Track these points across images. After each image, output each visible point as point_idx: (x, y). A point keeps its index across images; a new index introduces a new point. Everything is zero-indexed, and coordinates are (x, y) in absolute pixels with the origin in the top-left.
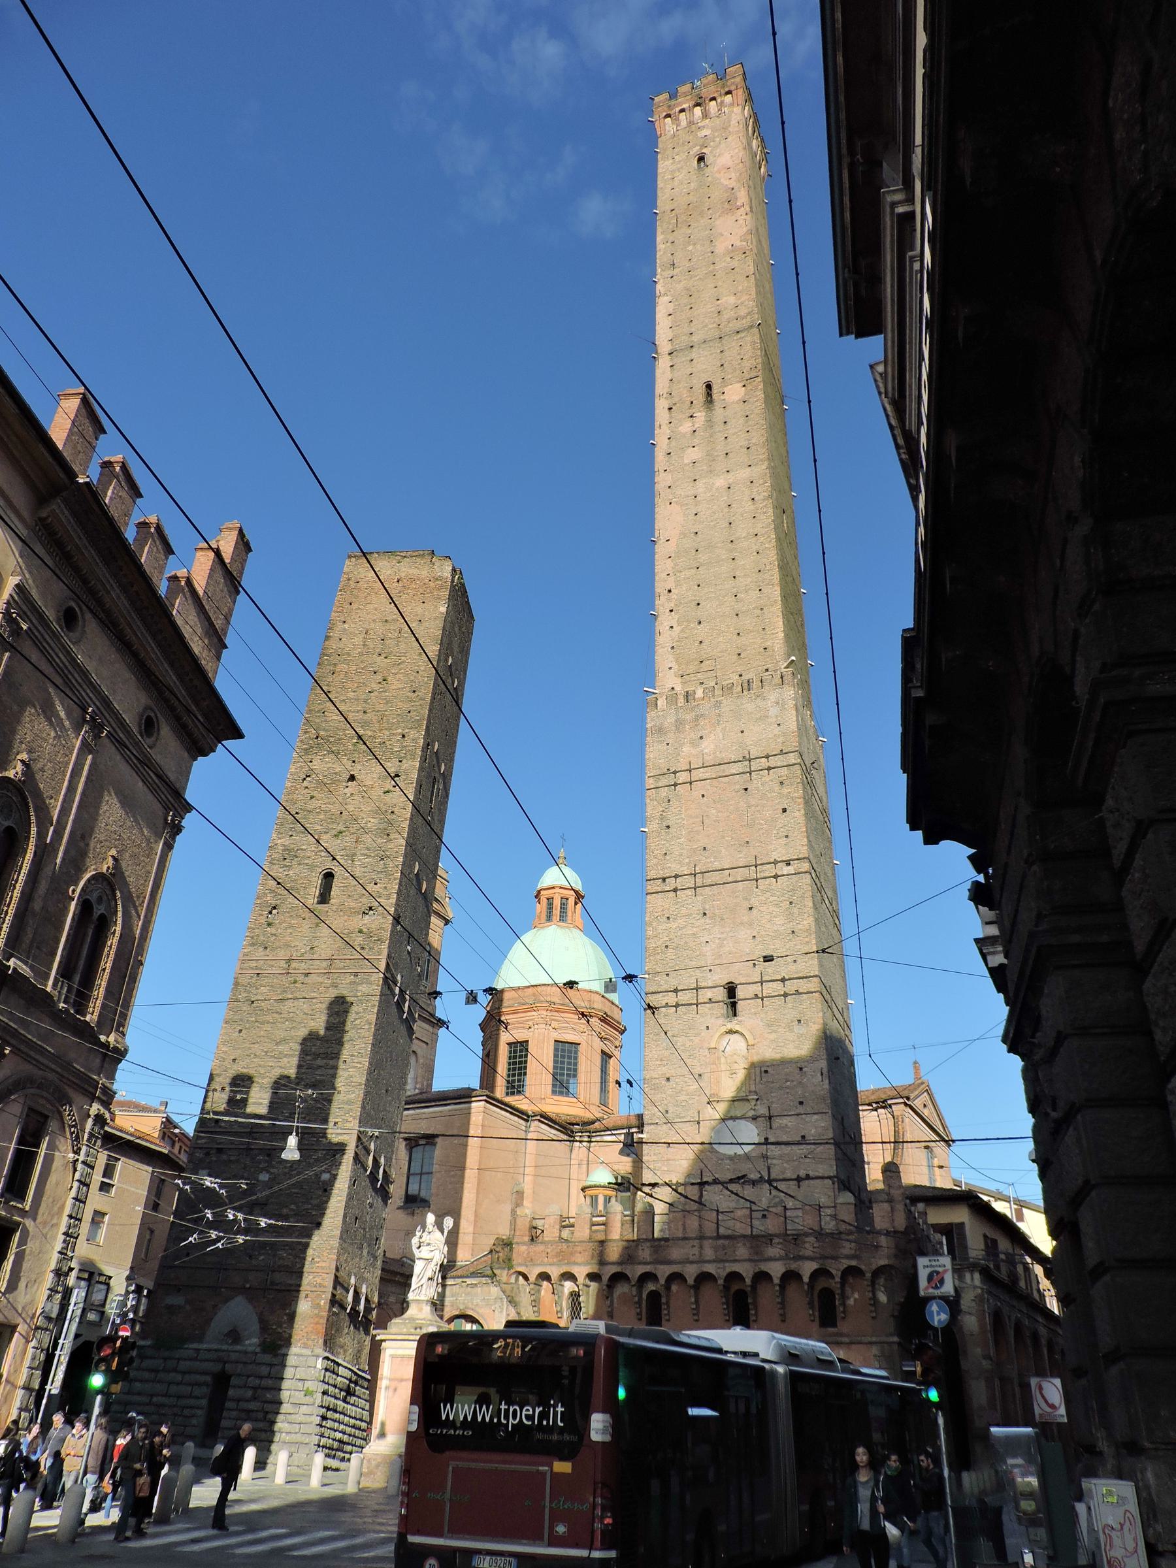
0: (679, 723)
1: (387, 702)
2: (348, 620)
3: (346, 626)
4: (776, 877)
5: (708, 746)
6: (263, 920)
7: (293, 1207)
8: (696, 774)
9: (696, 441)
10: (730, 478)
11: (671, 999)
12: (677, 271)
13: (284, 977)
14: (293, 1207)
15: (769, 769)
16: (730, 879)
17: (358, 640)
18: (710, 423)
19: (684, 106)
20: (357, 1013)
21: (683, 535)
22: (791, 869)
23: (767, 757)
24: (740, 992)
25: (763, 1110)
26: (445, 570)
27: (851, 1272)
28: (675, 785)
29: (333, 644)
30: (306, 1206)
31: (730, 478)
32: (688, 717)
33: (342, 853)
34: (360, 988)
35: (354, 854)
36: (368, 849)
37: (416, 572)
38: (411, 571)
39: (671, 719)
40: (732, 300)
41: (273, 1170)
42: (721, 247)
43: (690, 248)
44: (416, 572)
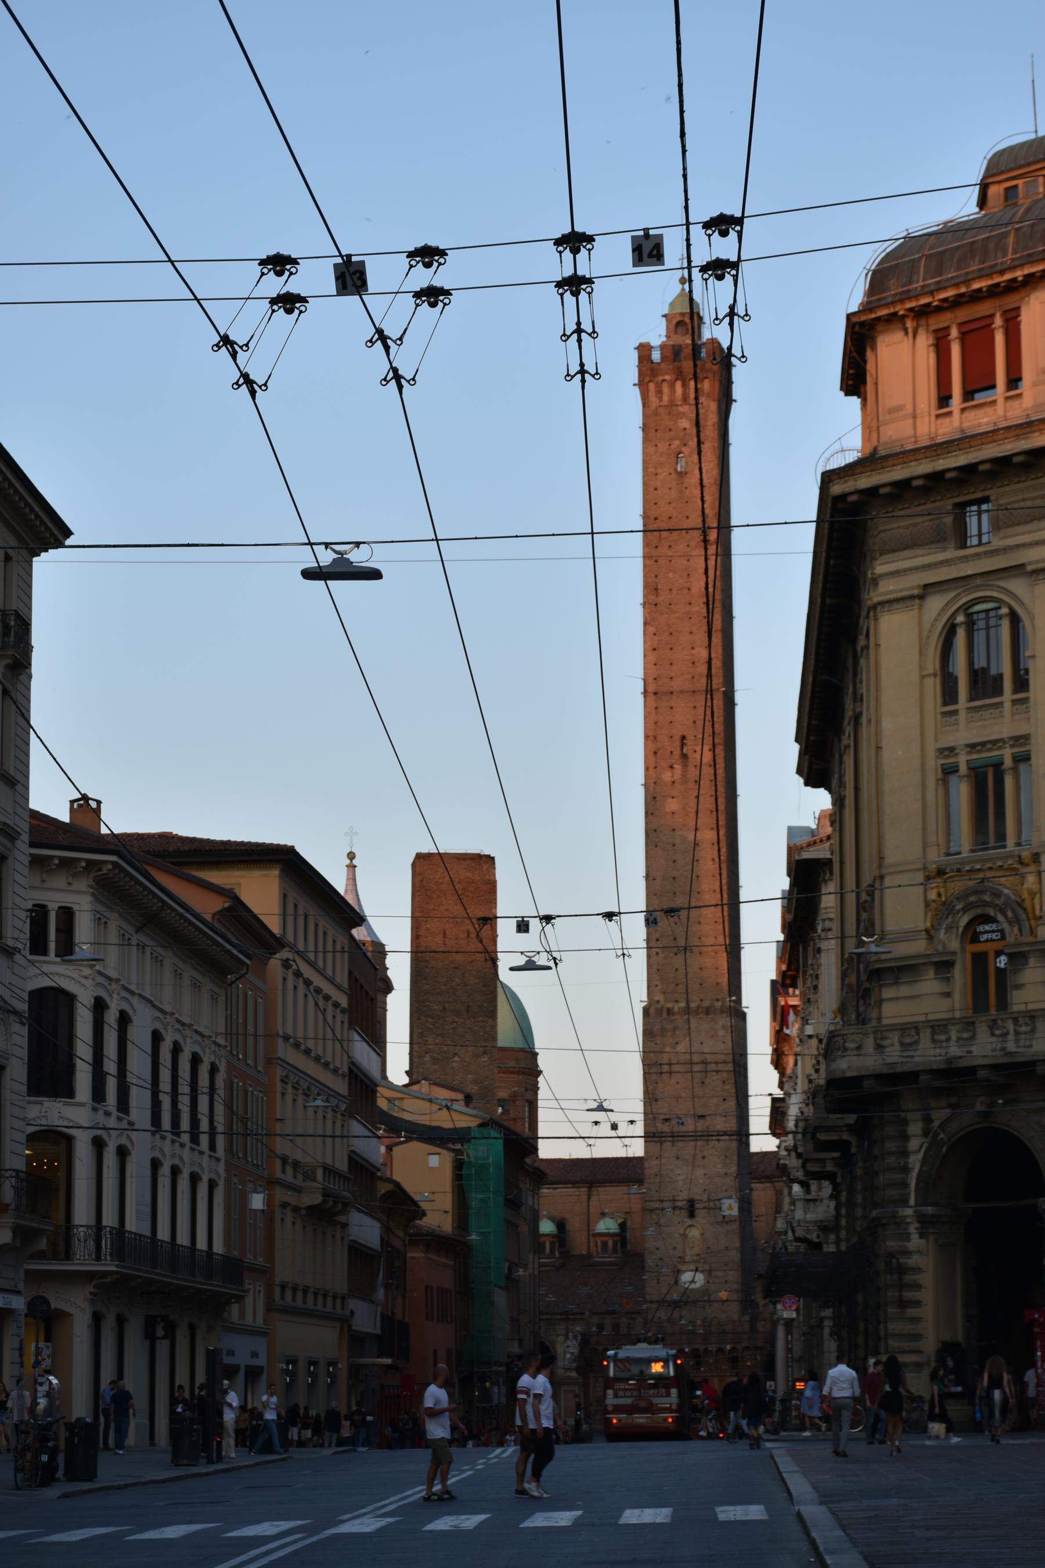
0: (663, 1030)
4: (719, 1140)
5: (681, 1048)
8: (676, 1068)
9: (675, 793)
12: (660, 599)
15: (717, 1071)
17: (439, 939)
19: (667, 377)
23: (717, 1063)
24: (697, 1206)
25: (707, 1267)
27: (747, 1348)
28: (661, 1073)
32: (669, 1027)
37: (469, 874)
39: (657, 1027)
43: (671, 575)
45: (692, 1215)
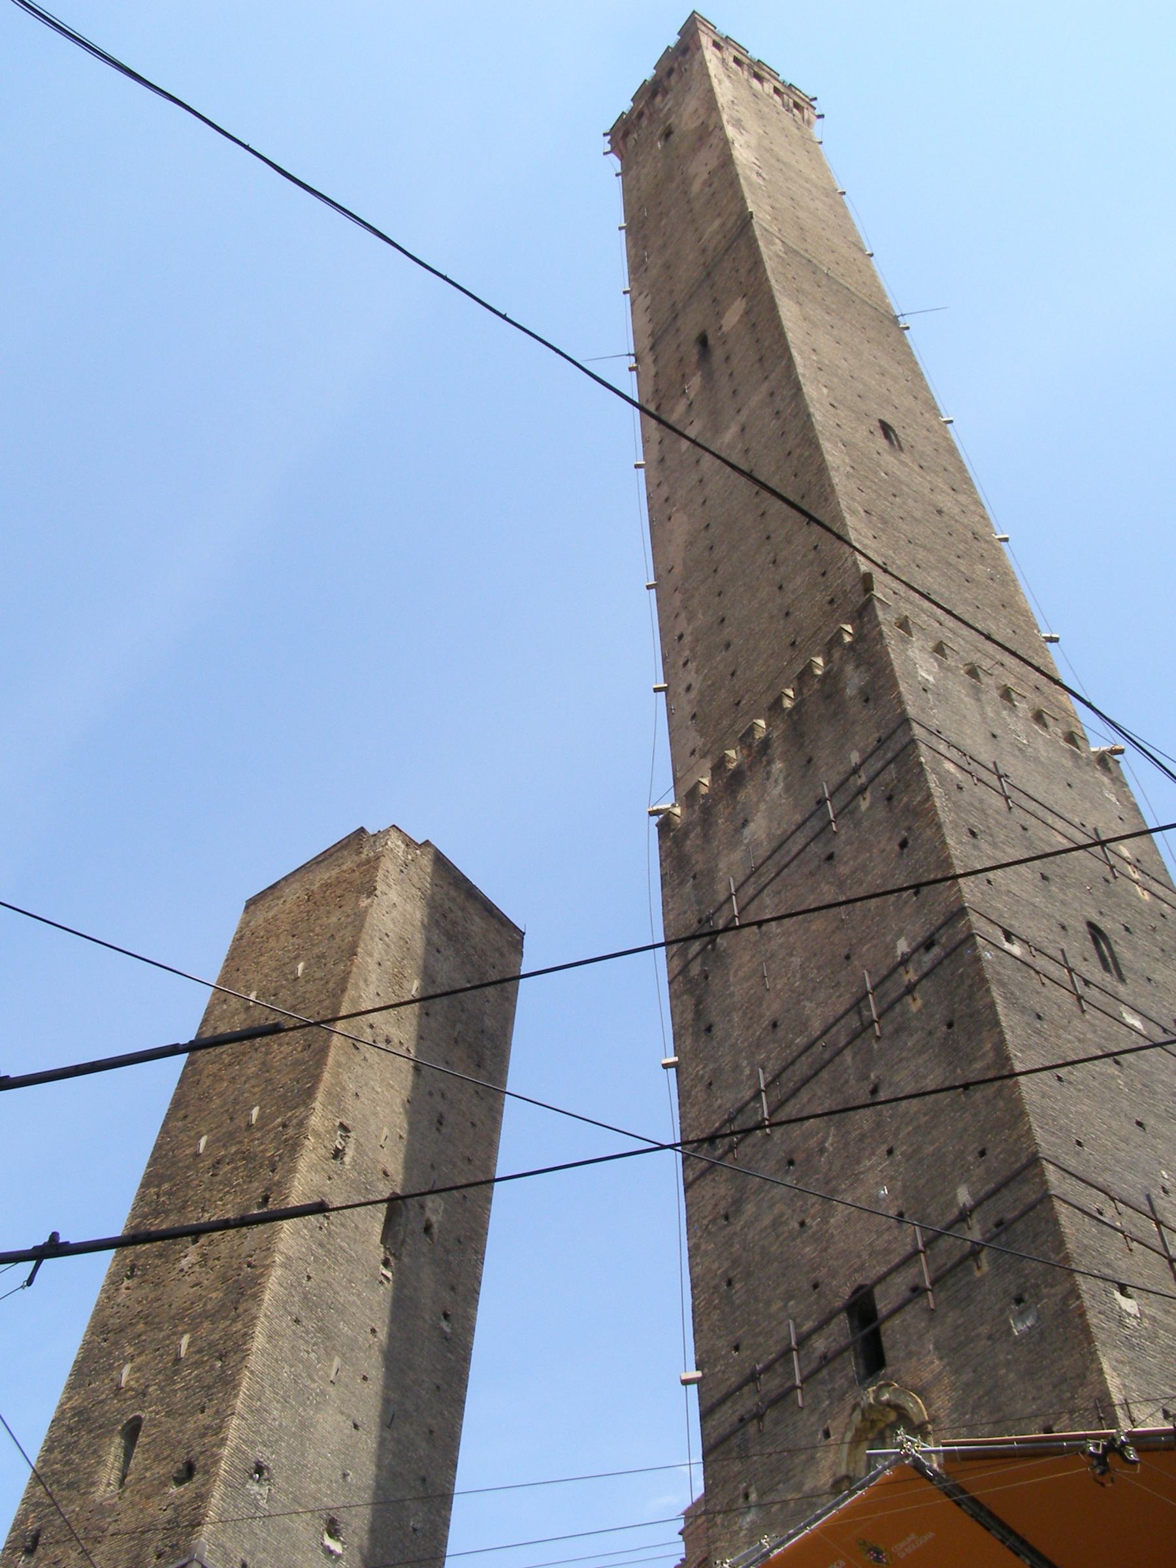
10: (742, 417)
11: (748, 1402)
18: (709, 377)
21: (690, 544)
22: (936, 951)
31: (742, 417)
36: (200, 1351)
40: (717, 223)
42: (696, 187)
45: (873, 1359)
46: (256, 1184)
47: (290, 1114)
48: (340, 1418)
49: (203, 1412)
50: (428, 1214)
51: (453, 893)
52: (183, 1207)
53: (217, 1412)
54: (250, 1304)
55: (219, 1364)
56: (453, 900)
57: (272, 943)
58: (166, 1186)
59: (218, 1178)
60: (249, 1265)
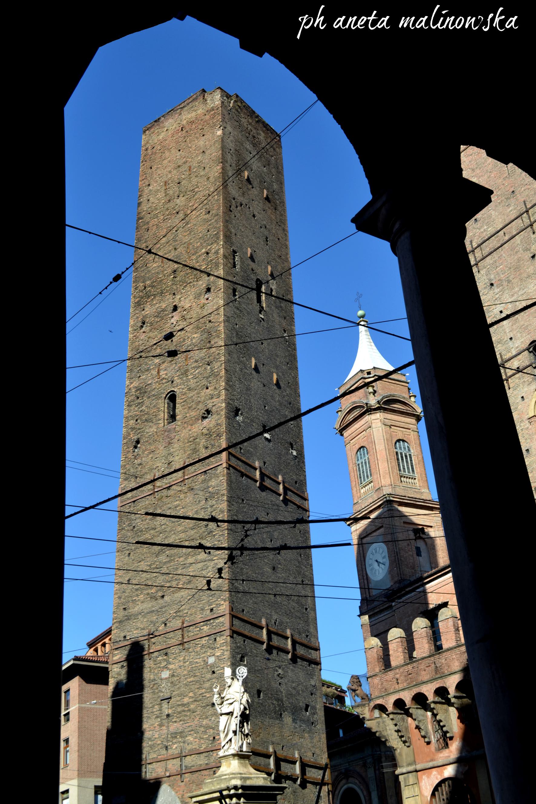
1: (190, 233)
2: (152, 182)
3: (151, 188)
6: (130, 455)
7: (191, 694)
13: (152, 496)
14: (191, 694)
16: (507, 238)
17: (161, 195)
20: (212, 506)
26: (216, 99)
29: (145, 207)
30: (201, 691)
33: (178, 373)
34: (210, 484)
35: (187, 371)
37: (193, 114)
38: (189, 116)
41: (171, 666)
44: (193, 114)
46: (201, 283)
47: (209, 247)
48: (259, 383)
49: (207, 388)
50: (271, 286)
51: (250, 121)
52: (162, 293)
53: (215, 388)
54: (216, 340)
55: (209, 367)
56: (250, 124)
57: (167, 154)
58: (148, 282)
59: (178, 279)
60: (210, 321)
